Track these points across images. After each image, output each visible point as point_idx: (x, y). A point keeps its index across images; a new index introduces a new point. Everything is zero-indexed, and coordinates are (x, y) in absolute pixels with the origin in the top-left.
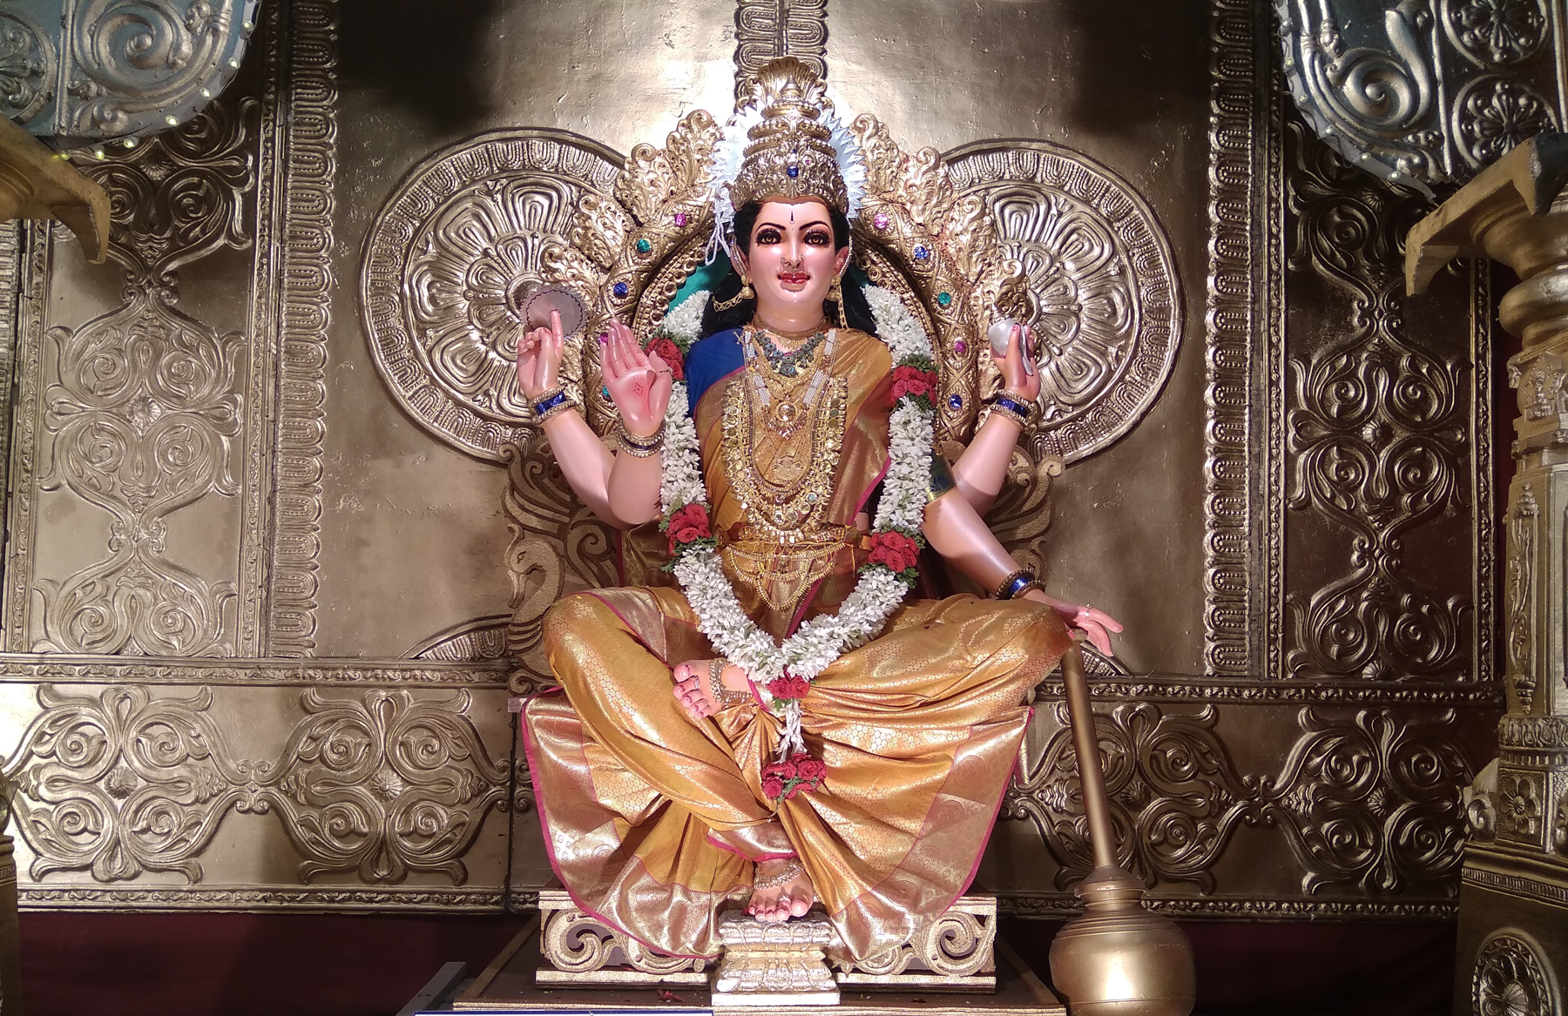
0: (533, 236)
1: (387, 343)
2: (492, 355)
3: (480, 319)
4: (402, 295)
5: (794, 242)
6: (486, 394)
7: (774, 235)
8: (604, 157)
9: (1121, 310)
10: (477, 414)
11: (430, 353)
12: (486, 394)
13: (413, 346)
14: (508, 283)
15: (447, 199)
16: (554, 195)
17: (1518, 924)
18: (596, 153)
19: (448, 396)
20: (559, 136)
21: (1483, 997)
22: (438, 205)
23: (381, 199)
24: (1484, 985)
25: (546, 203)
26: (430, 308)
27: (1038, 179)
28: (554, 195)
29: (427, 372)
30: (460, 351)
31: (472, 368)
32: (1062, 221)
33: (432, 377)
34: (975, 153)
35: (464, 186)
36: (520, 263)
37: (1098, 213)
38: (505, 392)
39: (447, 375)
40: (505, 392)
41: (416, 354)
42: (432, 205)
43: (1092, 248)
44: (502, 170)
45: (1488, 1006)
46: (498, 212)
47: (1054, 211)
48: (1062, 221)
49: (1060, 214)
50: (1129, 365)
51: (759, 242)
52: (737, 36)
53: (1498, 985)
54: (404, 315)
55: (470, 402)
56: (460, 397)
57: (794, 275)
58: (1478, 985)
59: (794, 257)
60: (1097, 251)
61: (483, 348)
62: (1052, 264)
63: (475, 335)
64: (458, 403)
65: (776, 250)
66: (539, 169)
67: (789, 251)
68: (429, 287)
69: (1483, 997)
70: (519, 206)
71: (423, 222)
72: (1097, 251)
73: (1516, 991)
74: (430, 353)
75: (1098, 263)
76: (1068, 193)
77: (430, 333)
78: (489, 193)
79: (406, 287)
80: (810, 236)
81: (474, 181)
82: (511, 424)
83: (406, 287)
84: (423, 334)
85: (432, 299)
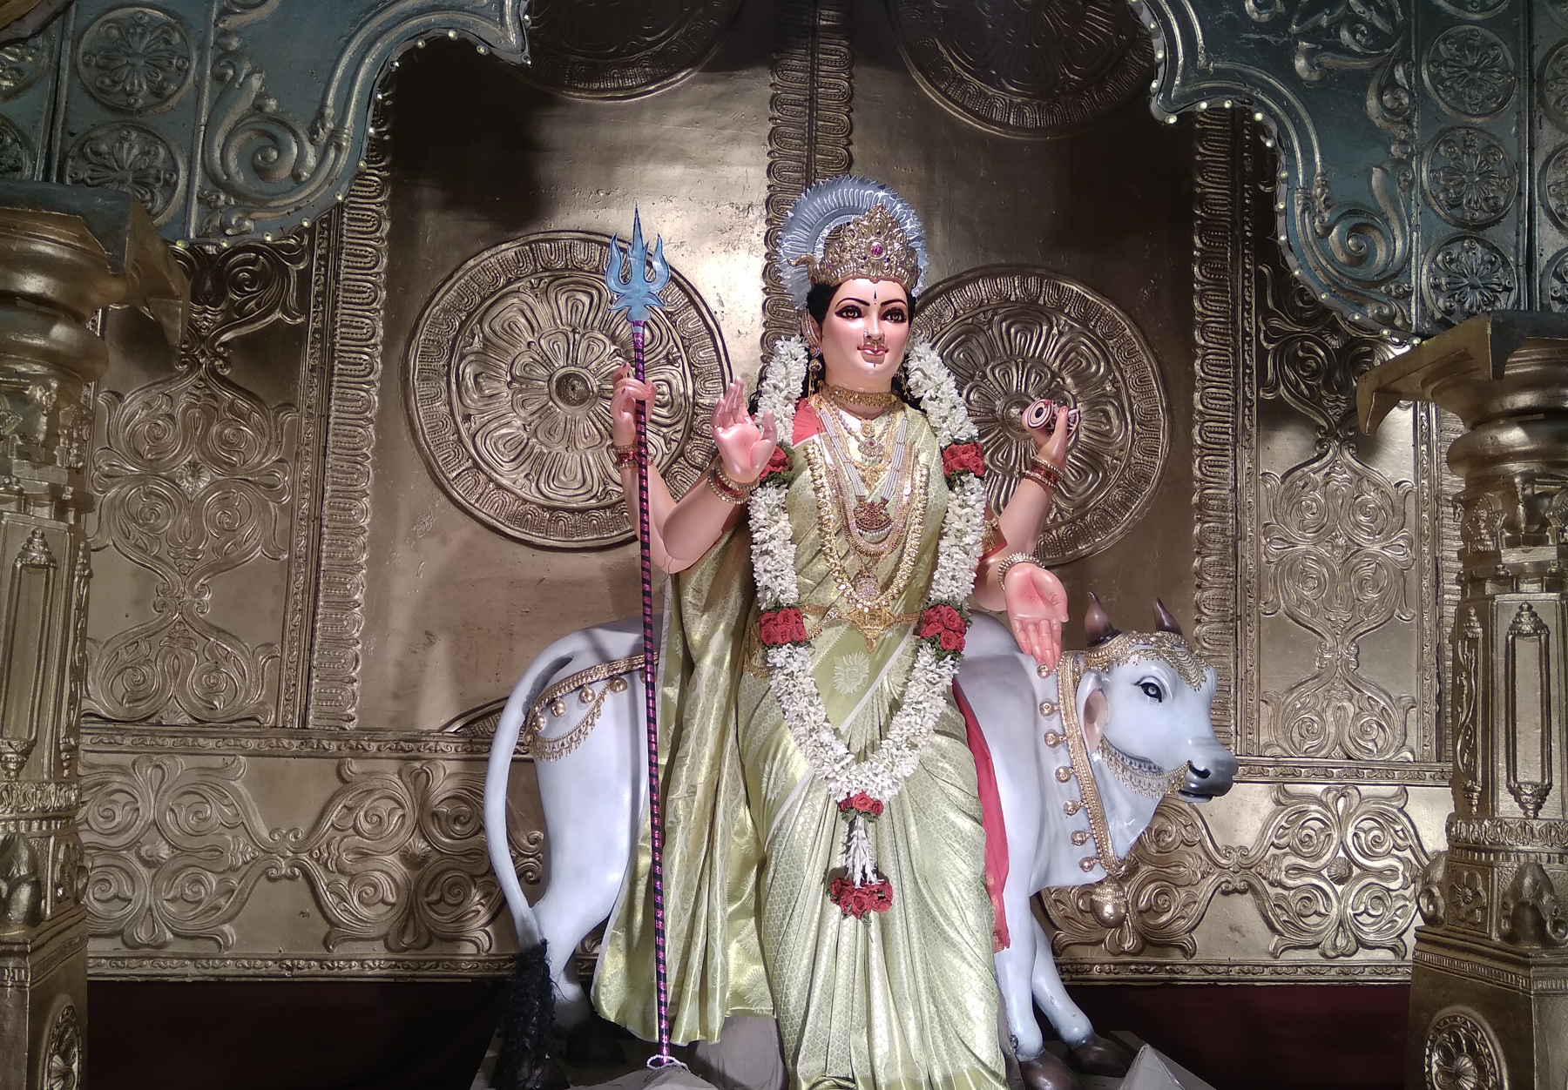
0: (574, 331)
9: (1115, 422)
13: (458, 431)
14: (551, 376)
15: (493, 294)
16: (594, 292)
17: (1469, 1004)
21: (1435, 1069)
22: (484, 300)
24: (1435, 1058)
25: (587, 300)
27: (1041, 302)
28: (594, 292)
29: (471, 457)
32: (1063, 340)
33: (475, 461)
34: (983, 277)
35: (509, 282)
37: (1095, 334)
41: (460, 440)
42: (478, 300)
43: (1089, 366)
45: (1440, 1077)
47: (1055, 331)
48: (1063, 340)
49: (1061, 333)
53: (1449, 1058)
58: (1430, 1057)
60: (1094, 368)
66: (581, 269)
69: (1435, 1069)
70: (562, 302)
71: (469, 316)
72: (1094, 368)
73: (1466, 1063)
76: (1068, 315)
81: (518, 279)
84: (467, 418)
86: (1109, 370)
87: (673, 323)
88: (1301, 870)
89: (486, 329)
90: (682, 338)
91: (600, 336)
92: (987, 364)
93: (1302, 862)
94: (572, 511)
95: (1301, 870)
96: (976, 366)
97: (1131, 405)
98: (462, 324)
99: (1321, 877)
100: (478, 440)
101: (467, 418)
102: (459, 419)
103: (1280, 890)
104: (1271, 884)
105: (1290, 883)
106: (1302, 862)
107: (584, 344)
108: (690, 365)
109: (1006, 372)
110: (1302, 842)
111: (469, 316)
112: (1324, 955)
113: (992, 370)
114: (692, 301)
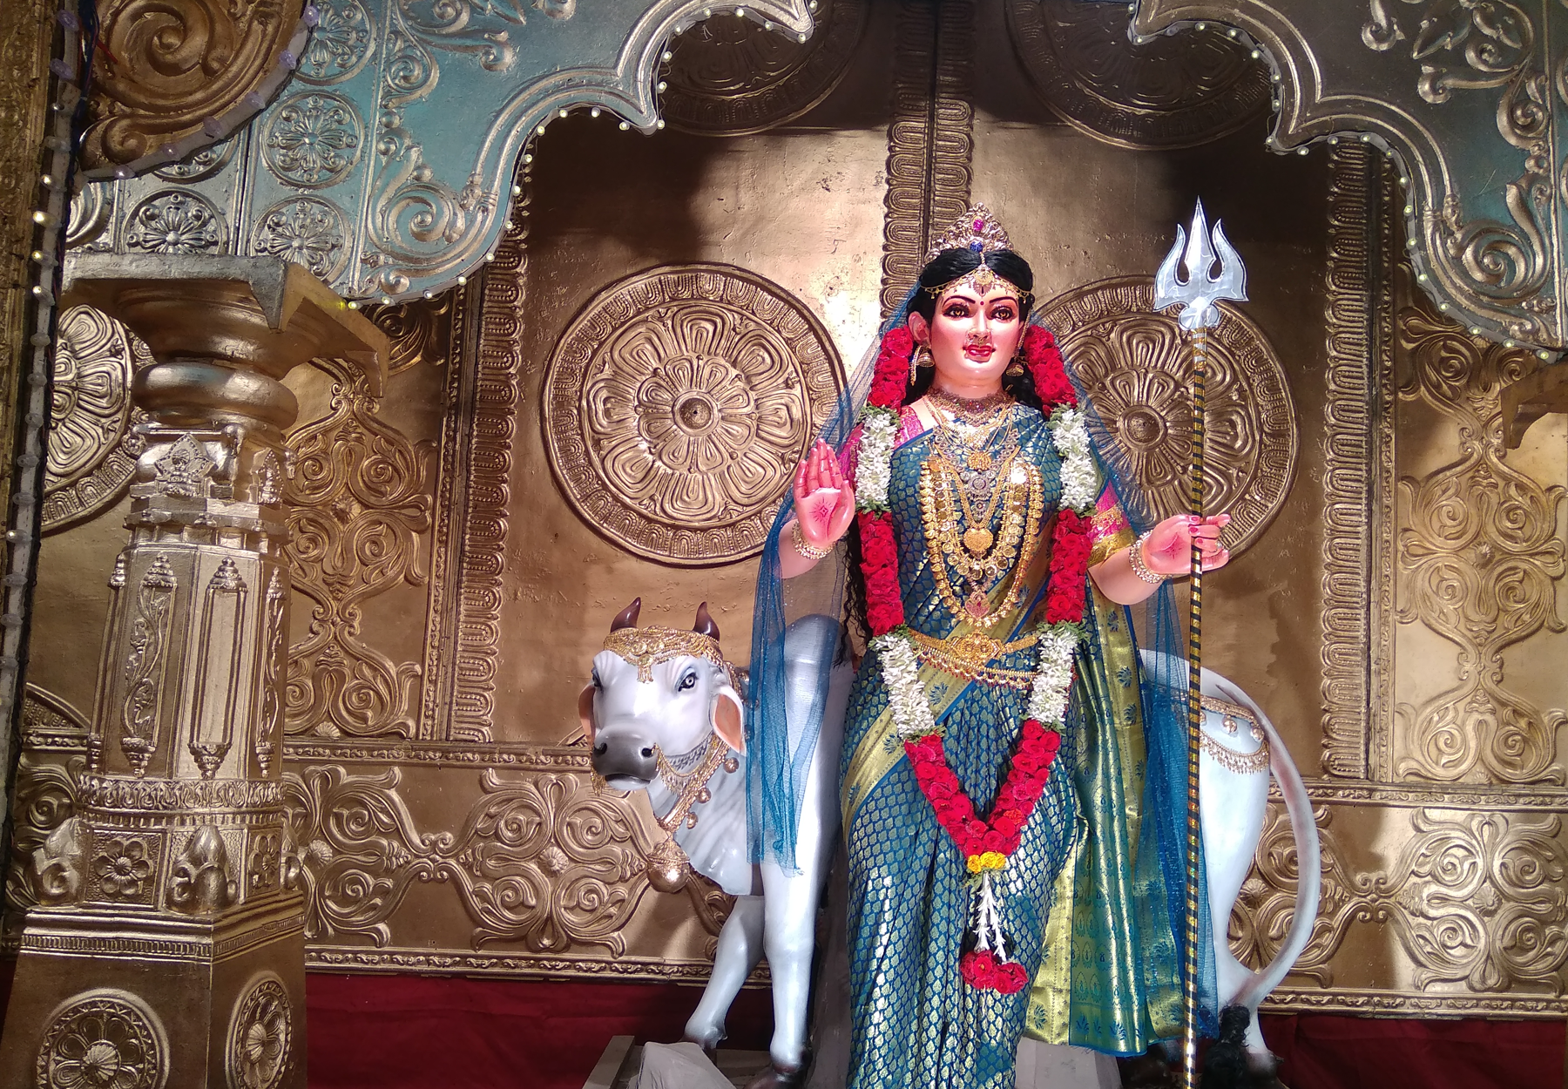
1: (565, 450)
2: (658, 463)
3: (649, 431)
4: (579, 409)
5: (981, 313)
6: (652, 498)
7: (961, 310)
8: (764, 289)
10: (641, 515)
11: (603, 461)
12: (652, 498)
14: (675, 400)
15: (623, 324)
16: (718, 321)
18: (757, 285)
19: (616, 498)
20: (723, 269)
22: (615, 329)
23: (563, 325)
25: (710, 328)
26: (604, 422)
28: (718, 321)
29: (598, 476)
30: (629, 460)
31: (640, 476)
33: (604, 483)
34: (1102, 288)
35: (639, 313)
36: (686, 382)
38: (668, 497)
39: (617, 481)
40: (668, 497)
41: (591, 463)
42: (609, 329)
44: (673, 299)
46: (668, 337)
47: (1178, 341)
50: (1249, 485)
51: (947, 314)
52: (888, 181)
54: (581, 427)
55: (637, 507)
56: (628, 500)
57: (980, 347)
59: (982, 329)
60: (1219, 377)
61: (651, 458)
62: (1177, 388)
63: (644, 446)
64: (626, 507)
65: (962, 325)
67: (977, 323)
68: (606, 401)
72: (1219, 377)
74: (603, 461)
75: (1221, 388)
77: (604, 443)
78: (661, 319)
79: (584, 403)
80: (998, 311)
81: (647, 309)
82: (673, 527)
83: (584, 403)
85: (607, 413)
86: (1235, 380)
87: (793, 349)
88: (1444, 900)
89: (616, 355)
90: (801, 363)
91: (723, 362)
92: (1106, 375)
93: (1444, 890)
94: (694, 530)
95: (1444, 900)
96: (1096, 379)
97: (1259, 414)
98: (595, 352)
99: (1468, 908)
100: (608, 464)
101: (597, 443)
102: (589, 444)
103: (1421, 920)
104: (1413, 914)
105: (1432, 913)
106: (1444, 890)
107: (707, 371)
108: (808, 389)
109: (1129, 384)
110: (1444, 871)
111: (601, 345)
112: (1472, 988)
113: (1112, 382)
114: (811, 328)
